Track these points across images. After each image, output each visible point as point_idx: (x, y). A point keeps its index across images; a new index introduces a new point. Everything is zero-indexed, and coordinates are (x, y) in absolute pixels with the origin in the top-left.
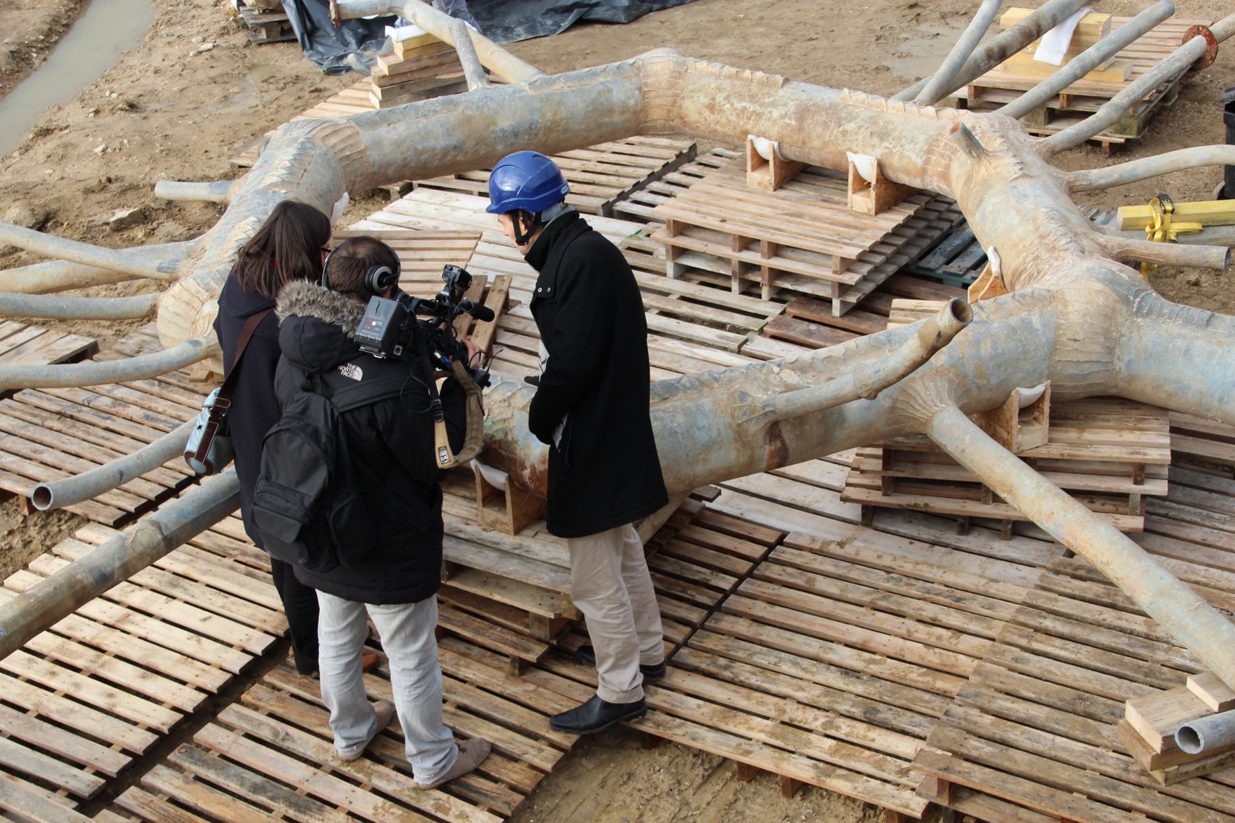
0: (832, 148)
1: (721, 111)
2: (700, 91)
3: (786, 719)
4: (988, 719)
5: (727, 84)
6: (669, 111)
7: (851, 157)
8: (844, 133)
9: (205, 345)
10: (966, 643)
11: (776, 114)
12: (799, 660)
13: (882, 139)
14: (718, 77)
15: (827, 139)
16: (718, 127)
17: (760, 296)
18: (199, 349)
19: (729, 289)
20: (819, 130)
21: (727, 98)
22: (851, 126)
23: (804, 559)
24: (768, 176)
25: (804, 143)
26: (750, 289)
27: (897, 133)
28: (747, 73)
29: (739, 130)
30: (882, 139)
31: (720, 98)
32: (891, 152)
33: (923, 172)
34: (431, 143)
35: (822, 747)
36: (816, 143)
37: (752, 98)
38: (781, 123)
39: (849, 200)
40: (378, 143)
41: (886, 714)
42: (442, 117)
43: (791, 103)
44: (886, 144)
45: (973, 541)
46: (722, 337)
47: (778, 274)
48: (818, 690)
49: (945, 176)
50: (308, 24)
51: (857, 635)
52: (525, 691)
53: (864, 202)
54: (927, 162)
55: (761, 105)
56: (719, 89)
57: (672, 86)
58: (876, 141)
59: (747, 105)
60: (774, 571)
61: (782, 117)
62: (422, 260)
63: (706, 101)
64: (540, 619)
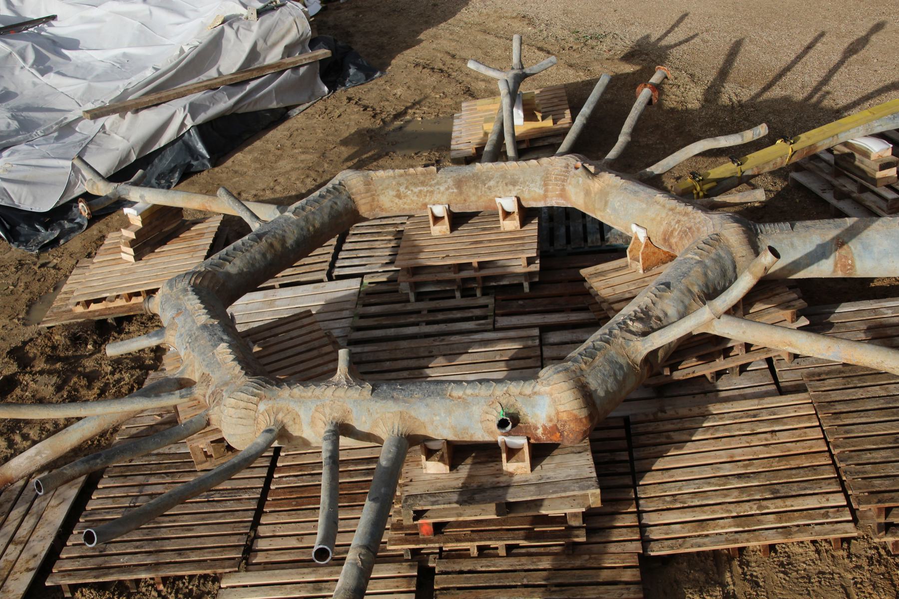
0: (484, 199)
1: (406, 196)
2: (387, 188)
4: (868, 467)
5: (402, 180)
6: (371, 205)
7: (498, 200)
8: (489, 188)
9: (277, 430)
10: (783, 437)
12: (708, 480)
13: (514, 185)
14: (394, 178)
15: (480, 194)
16: (406, 206)
17: (475, 295)
18: (274, 434)
19: (454, 297)
20: (473, 190)
21: (407, 188)
22: (492, 183)
23: (652, 427)
24: (443, 228)
25: (465, 200)
26: (467, 293)
27: (521, 179)
28: (411, 170)
30: (514, 185)
31: (402, 189)
32: (522, 191)
33: (545, 197)
34: (257, 265)
35: (770, 522)
36: (473, 198)
37: (423, 183)
38: (447, 192)
40: (228, 275)
41: (783, 491)
44: (517, 188)
45: (722, 384)
46: (479, 325)
47: (486, 279)
48: (736, 493)
49: (563, 194)
51: (724, 457)
53: (512, 224)
54: (546, 191)
55: (431, 186)
56: (399, 184)
57: (368, 191)
58: (511, 187)
59: (422, 188)
60: (644, 440)
61: (447, 189)
62: (292, 339)
63: (394, 193)
64: (575, 515)
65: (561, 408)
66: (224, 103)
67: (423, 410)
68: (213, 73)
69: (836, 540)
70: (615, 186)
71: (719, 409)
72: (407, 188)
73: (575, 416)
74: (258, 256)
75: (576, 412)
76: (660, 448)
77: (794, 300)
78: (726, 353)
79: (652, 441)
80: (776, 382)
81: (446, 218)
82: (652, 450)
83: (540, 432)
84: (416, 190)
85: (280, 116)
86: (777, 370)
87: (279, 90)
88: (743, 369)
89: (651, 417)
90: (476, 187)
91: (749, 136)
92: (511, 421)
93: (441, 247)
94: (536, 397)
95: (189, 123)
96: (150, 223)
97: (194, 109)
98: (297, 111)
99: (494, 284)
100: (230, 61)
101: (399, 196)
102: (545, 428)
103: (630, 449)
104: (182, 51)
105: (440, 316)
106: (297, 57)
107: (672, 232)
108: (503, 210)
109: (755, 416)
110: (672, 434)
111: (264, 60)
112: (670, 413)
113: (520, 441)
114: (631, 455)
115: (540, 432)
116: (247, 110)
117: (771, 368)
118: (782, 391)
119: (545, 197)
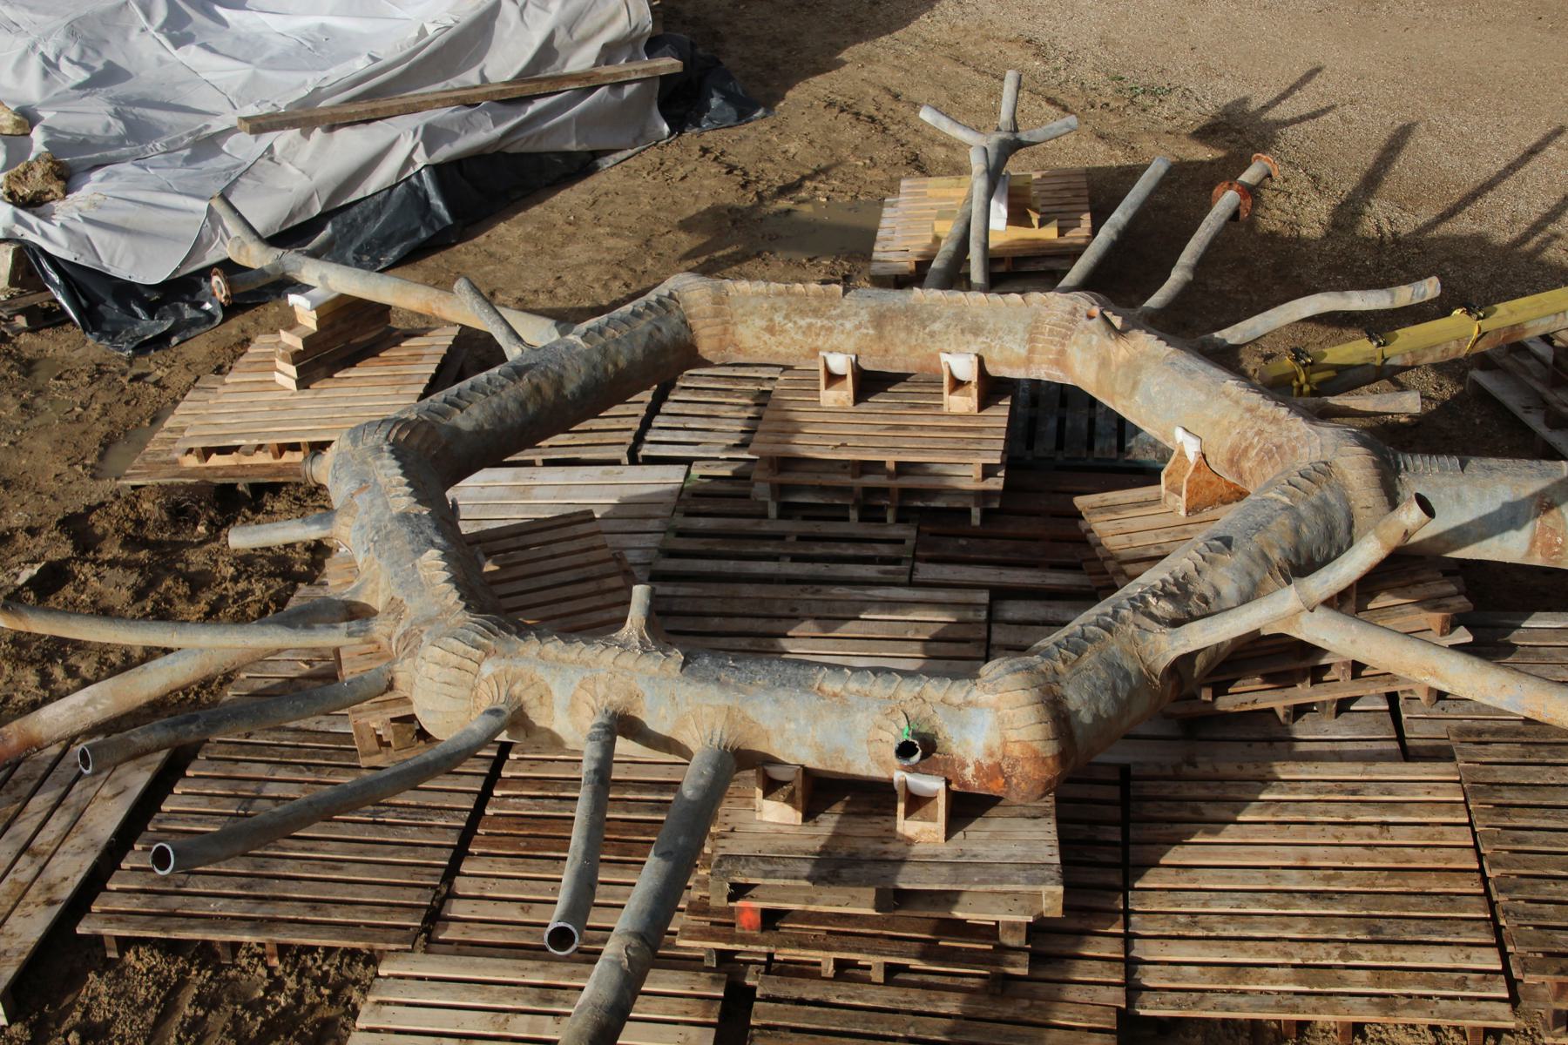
1: (783, 331)
3: (1297, 961)
4: (1550, 908)
5: (780, 302)
7: (944, 358)
8: (932, 335)
9: (508, 713)
10: (1400, 836)
11: (849, 325)
12: (1258, 895)
14: (767, 296)
15: (913, 342)
16: (782, 349)
17: (884, 520)
18: (503, 718)
19: (847, 519)
20: (903, 335)
21: (787, 317)
22: (937, 326)
23: (1168, 789)
24: (842, 395)
26: (871, 514)
28: (799, 287)
29: (806, 348)
31: (778, 318)
32: (990, 347)
33: (1028, 361)
34: (509, 421)
36: (901, 349)
37: (816, 312)
38: (857, 333)
39: (945, 402)
40: (456, 432)
42: (511, 389)
43: (863, 312)
44: (981, 339)
45: (1302, 729)
46: (885, 572)
47: (907, 493)
48: (1304, 924)
49: (1060, 361)
50: (83, 302)
52: (1024, 1009)
53: (963, 403)
54: (1031, 351)
56: (774, 309)
58: (969, 337)
60: (1150, 809)
61: (858, 327)
62: (553, 557)
63: (764, 323)
64: (1013, 927)
65: (1013, 735)
66: (484, 132)
67: (769, 709)
68: (471, 77)
69: (1474, 1030)
70: (1155, 357)
71: (1292, 772)
72: (787, 317)
73: (1036, 752)
74: (512, 406)
75: (1038, 746)
76: (1179, 828)
77: (1451, 595)
78: (1317, 674)
79: (1166, 814)
80: (1401, 738)
81: (850, 379)
82: (1165, 830)
83: (969, 772)
84: (803, 323)
85: (581, 166)
86: (1404, 716)
87: (581, 119)
88: (1343, 706)
89: (1170, 772)
90: (909, 329)
91: (1404, 295)
92: (920, 747)
93: (833, 428)
94: (970, 710)
95: (421, 159)
96: (332, 326)
97: (431, 137)
98: (610, 160)
99: (919, 504)
100: (504, 61)
101: (771, 330)
102: (979, 766)
103: (1124, 823)
104: (423, 32)
105: (818, 550)
106: (622, 66)
107: (1246, 450)
108: (952, 376)
109: (1354, 793)
110: (1202, 805)
111: (564, 64)
112: (1204, 768)
113: (932, 784)
114: (1125, 834)
115: (969, 772)
116: (524, 149)
117: (1394, 712)
118: (1408, 754)
119: (1028, 361)
